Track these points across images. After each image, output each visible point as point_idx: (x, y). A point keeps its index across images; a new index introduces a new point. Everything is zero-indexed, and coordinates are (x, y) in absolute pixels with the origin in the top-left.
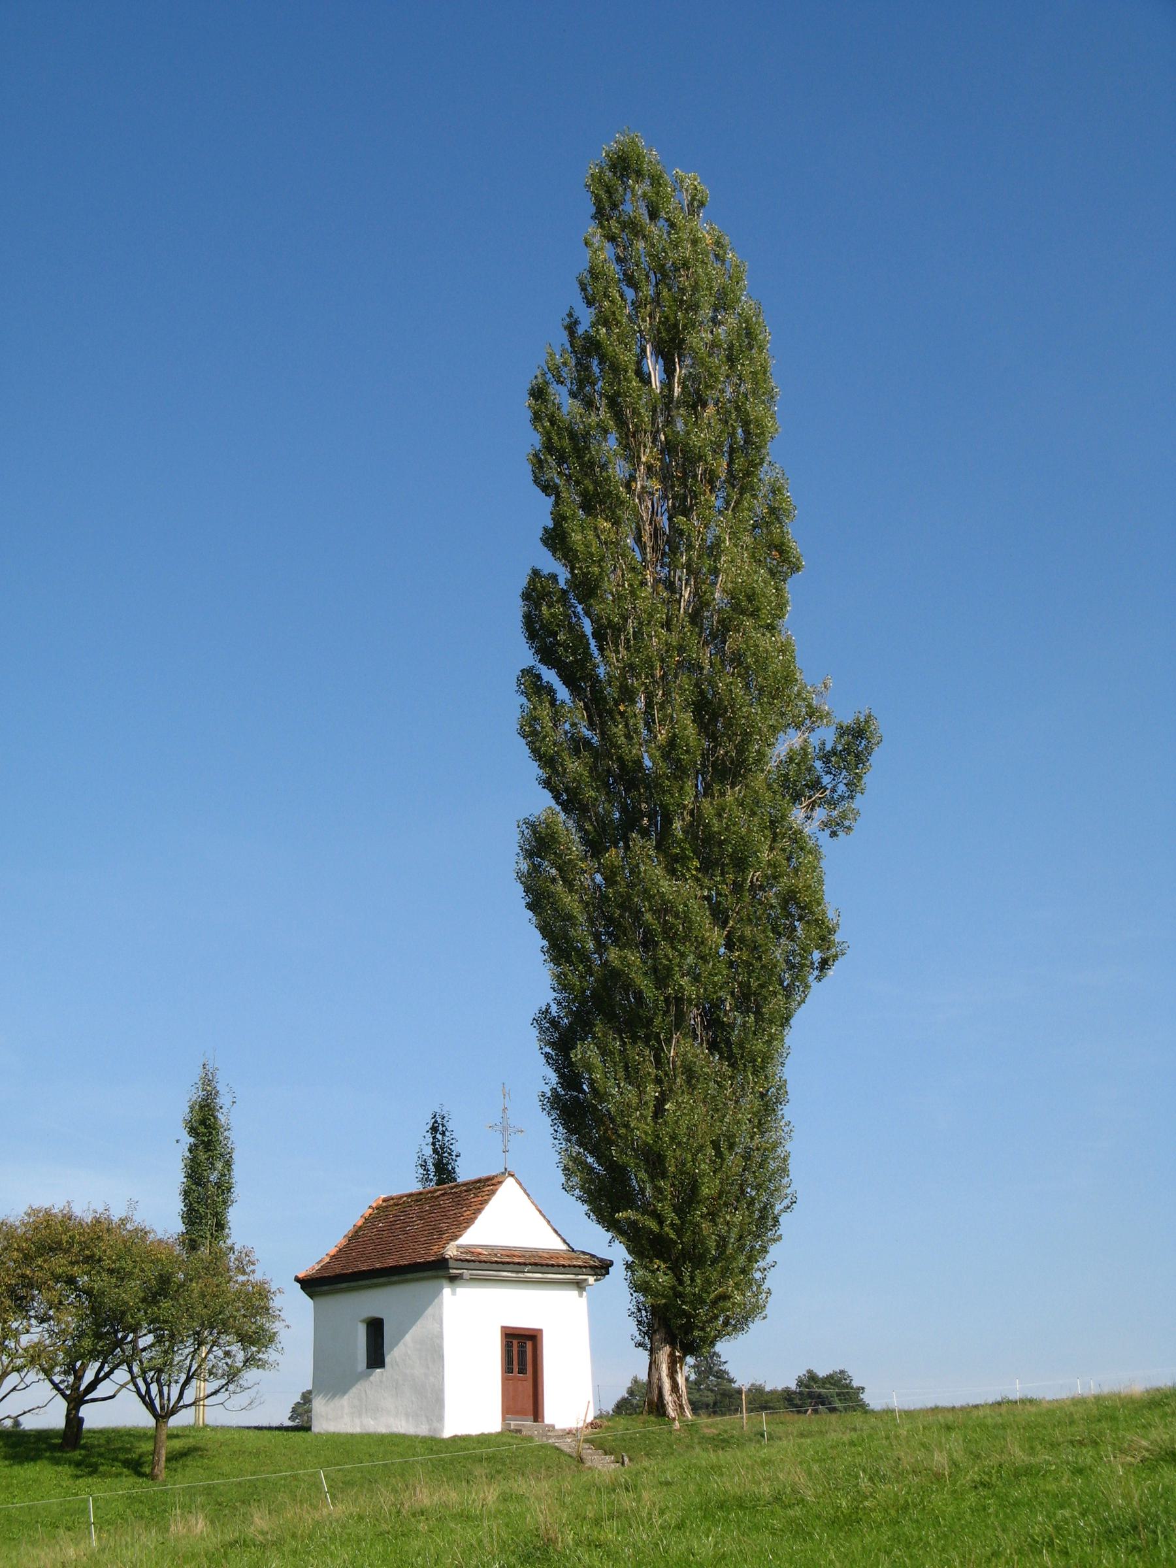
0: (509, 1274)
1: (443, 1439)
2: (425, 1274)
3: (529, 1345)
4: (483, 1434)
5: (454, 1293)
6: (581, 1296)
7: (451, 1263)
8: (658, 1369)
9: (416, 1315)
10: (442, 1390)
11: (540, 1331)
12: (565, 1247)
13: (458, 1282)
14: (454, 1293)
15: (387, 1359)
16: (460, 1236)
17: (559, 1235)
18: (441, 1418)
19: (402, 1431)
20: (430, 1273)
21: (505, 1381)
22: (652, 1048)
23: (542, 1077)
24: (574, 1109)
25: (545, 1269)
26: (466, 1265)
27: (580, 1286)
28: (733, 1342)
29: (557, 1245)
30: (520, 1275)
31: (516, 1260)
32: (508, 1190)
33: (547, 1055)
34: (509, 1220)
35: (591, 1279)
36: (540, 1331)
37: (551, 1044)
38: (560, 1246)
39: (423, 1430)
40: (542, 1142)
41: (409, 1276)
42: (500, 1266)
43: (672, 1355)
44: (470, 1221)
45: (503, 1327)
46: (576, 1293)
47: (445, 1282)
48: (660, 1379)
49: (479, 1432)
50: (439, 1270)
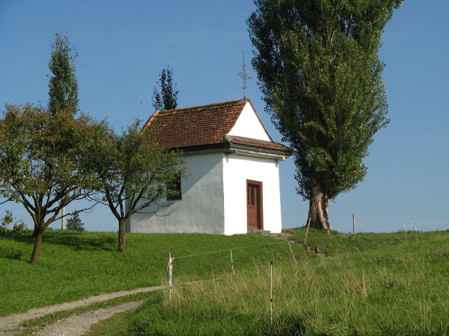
0: (253, 152)
1: (225, 236)
2: (213, 150)
3: (255, 189)
4: (235, 235)
5: (227, 161)
6: (276, 166)
7: (231, 145)
8: (317, 205)
9: (203, 173)
10: (223, 211)
11: (261, 183)
12: (269, 140)
13: (229, 155)
14: (227, 161)
15: (183, 196)
16: (230, 131)
17: (268, 134)
18: (222, 226)
19: (193, 232)
20: (216, 150)
21: (248, 207)
22: (323, 37)
23: (251, 52)
24: (267, 70)
25: (267, 151)
26: (237, 146)
27: (276, 160)
28: (348, 193)
29: (266, 138)
30: (257, 153)
31: (254, 145)
32: (248, 109)
33: (253, 40)
34: (249, 125)
35: (284, 157)
36: (261, 183)
37: (256, 33)
38: (268, 140)
39: (209, 231)
40: (254, 85)
41: (201, 151)
42: (249, 148)
43: (323, 198)
44: (232, 123)
45: (248, 180)
46: (274, 164)
47: (224, 155)
48: (317, 210)
49: (233, 234)
50: (226, 148)
